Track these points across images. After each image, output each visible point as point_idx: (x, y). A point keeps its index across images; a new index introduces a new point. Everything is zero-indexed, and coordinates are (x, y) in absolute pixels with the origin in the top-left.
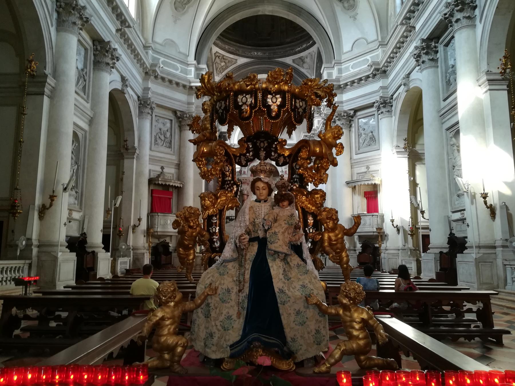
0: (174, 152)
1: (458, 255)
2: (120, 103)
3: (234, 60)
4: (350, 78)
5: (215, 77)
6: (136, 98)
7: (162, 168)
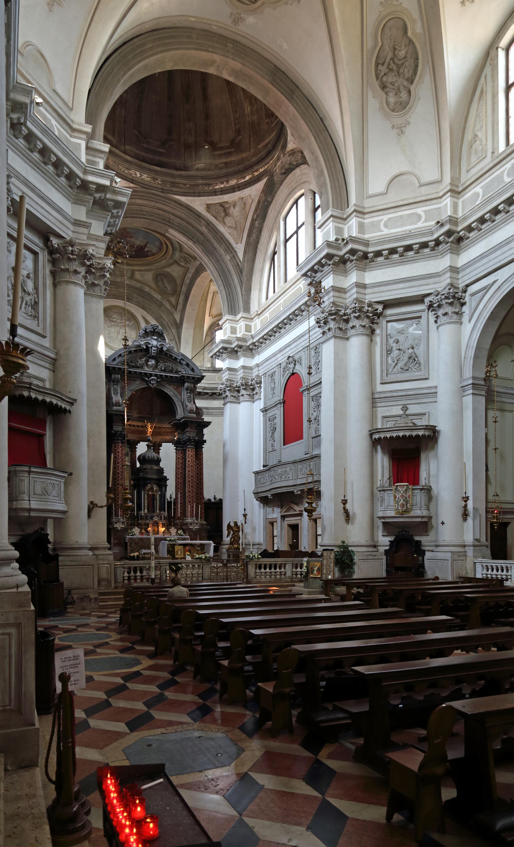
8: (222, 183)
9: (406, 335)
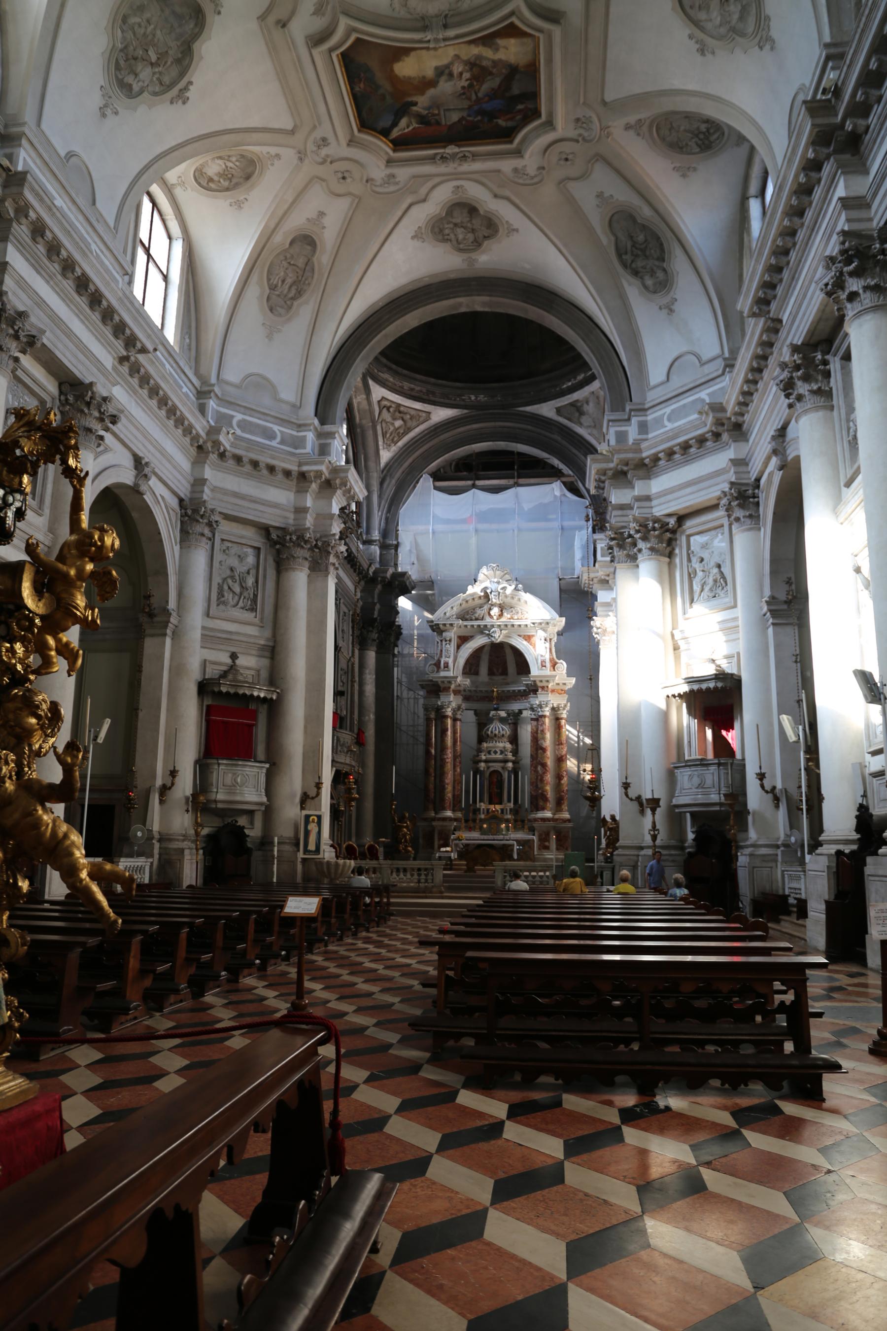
0: (262, 620)
1: (869, 860)
2: (135, 515)
3: (424, 415)
4: (662, 442)
5: (382, 452)
6: (174, 503)
7: (234, 656)
8: (570, 381)
9: (710, 551)
